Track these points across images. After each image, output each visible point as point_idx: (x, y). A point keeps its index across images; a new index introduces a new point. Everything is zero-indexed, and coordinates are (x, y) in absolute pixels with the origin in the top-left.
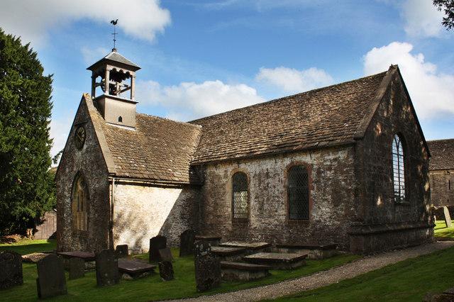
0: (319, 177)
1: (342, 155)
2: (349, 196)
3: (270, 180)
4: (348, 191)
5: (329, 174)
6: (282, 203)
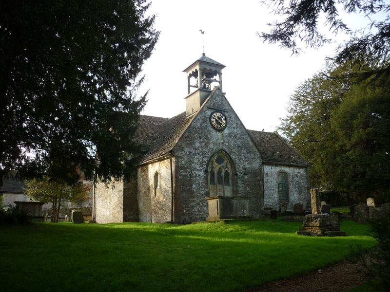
1: (302, 171)
2: (305, 190)
3: (269, 178)
4: (305, 187)
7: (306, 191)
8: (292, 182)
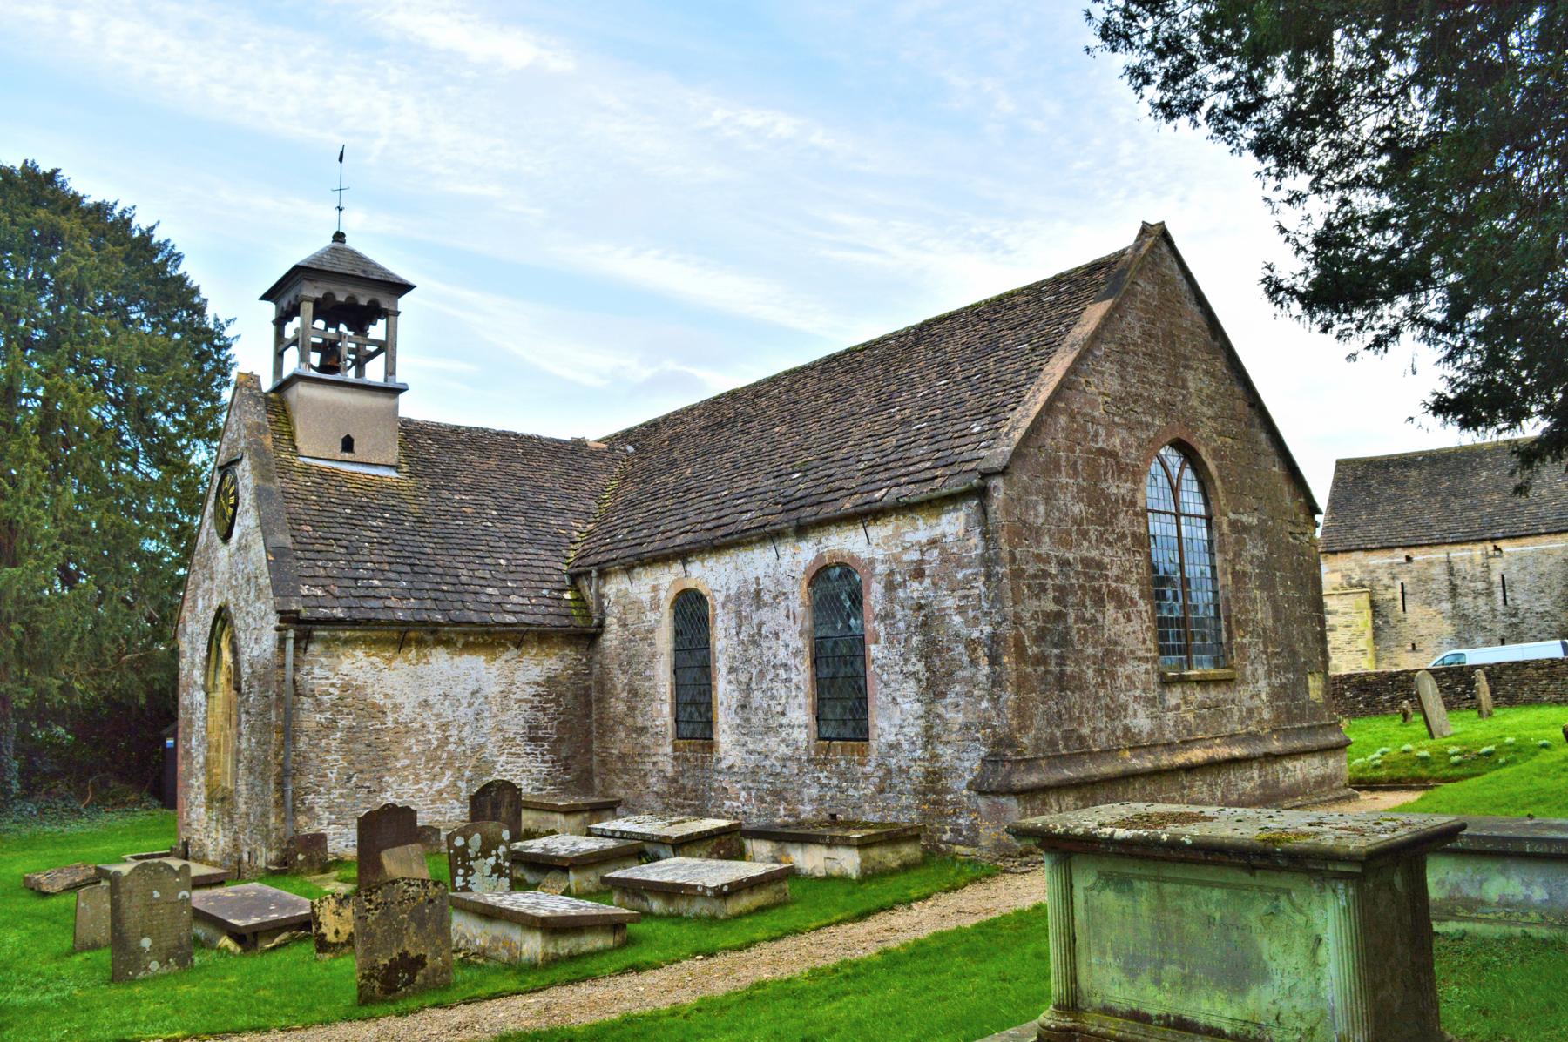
0: (891, 601)
1: (952, 524)
2: (974, 663)
3: (765, 614)
4: (971, 645)
5: (915, 589)
6: (798, 688)
7: (985, 669)
8: (887, 616)
